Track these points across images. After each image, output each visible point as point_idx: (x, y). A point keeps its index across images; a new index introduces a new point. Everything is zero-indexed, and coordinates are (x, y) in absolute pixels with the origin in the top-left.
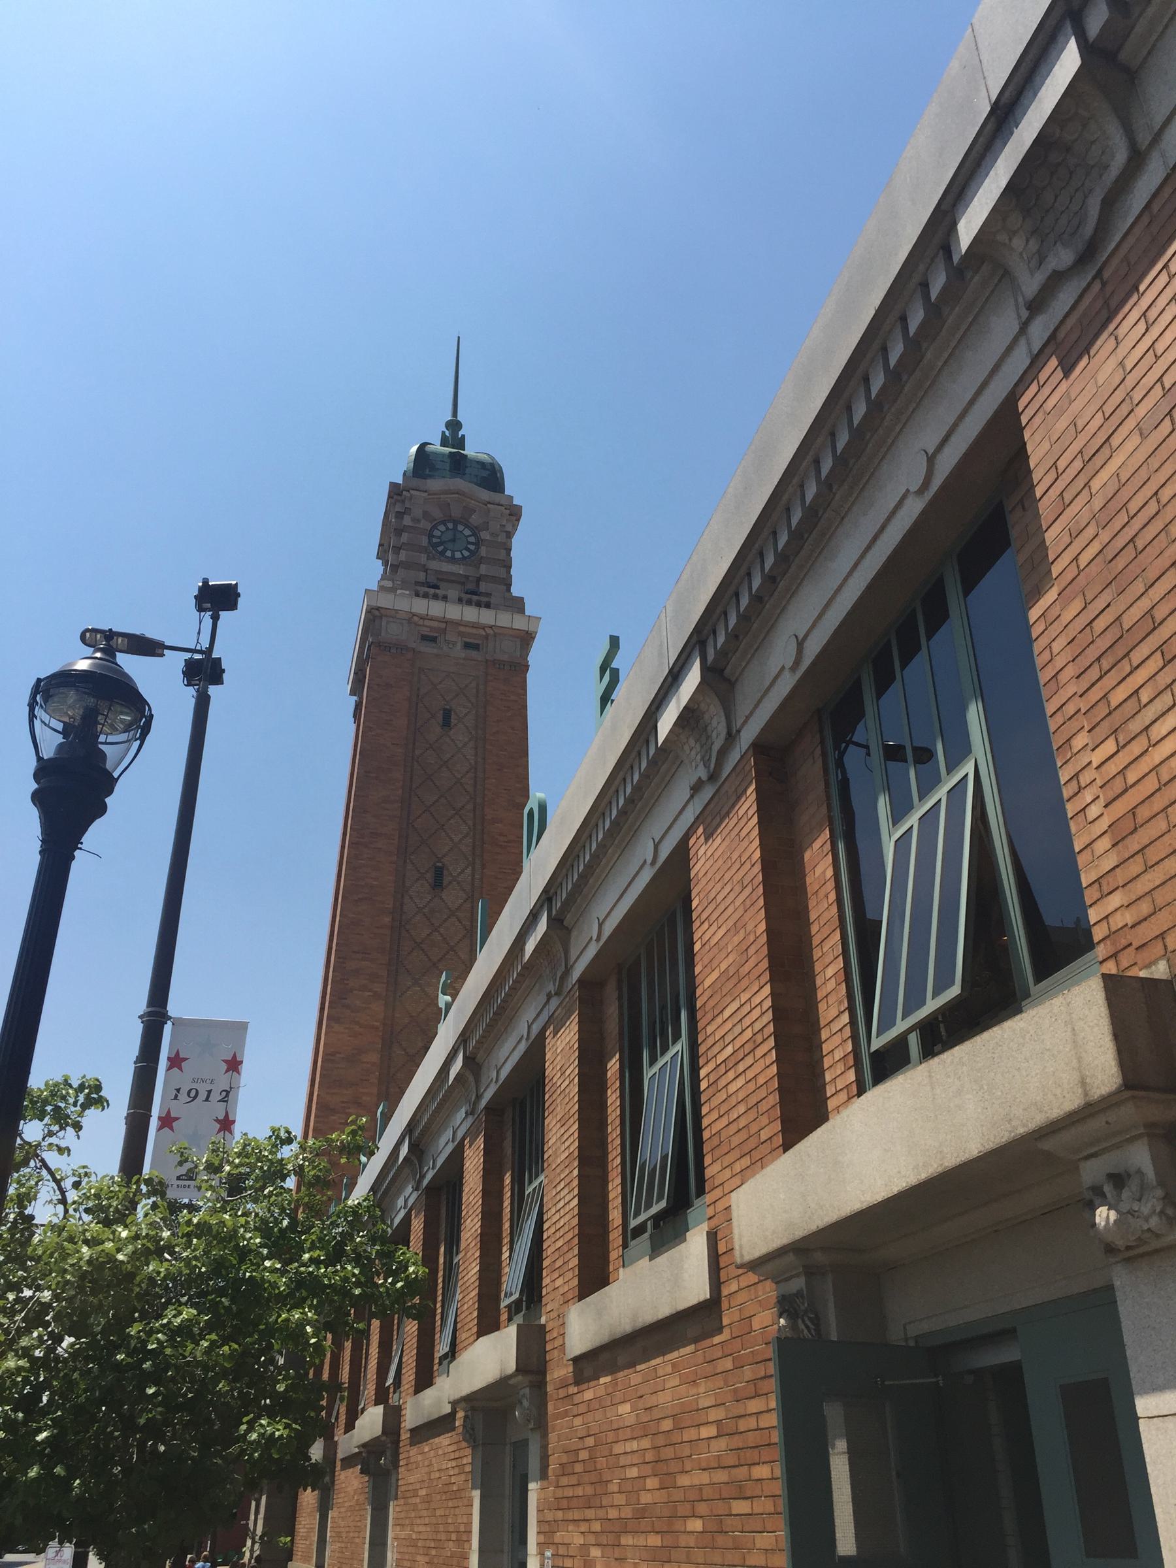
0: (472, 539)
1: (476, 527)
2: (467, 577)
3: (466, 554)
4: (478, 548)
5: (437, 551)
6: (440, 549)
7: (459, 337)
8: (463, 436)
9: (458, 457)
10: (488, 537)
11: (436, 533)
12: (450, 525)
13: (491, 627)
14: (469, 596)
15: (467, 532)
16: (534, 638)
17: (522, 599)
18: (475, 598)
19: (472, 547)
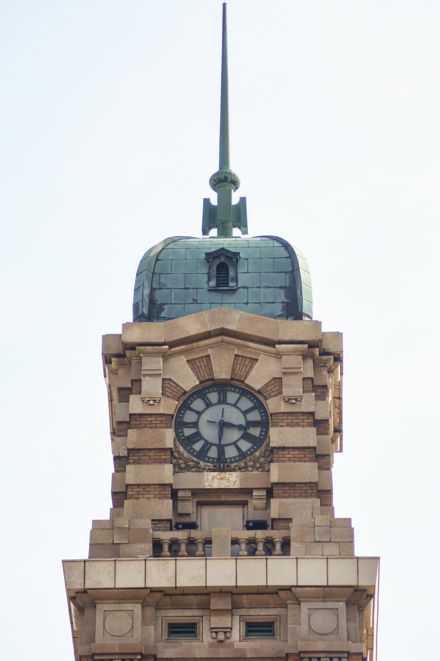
0: (255, 416)
1: (259, 392)
2: (248, 492)
3: (245, 446)
4: (265, 434)
5: (191, 451)
6: (198, 446)
7: (224, 5)
8: (243, 200)
9: (222, 259)
10: (283, 408)
11: (189, 417)
12: (213, 397)
13: (288, 589)
14: (251, 534)
15: (246, 404)
16: (371, 596)
17: (349, 520)
18: (260, 534)
19: (255, 432)
